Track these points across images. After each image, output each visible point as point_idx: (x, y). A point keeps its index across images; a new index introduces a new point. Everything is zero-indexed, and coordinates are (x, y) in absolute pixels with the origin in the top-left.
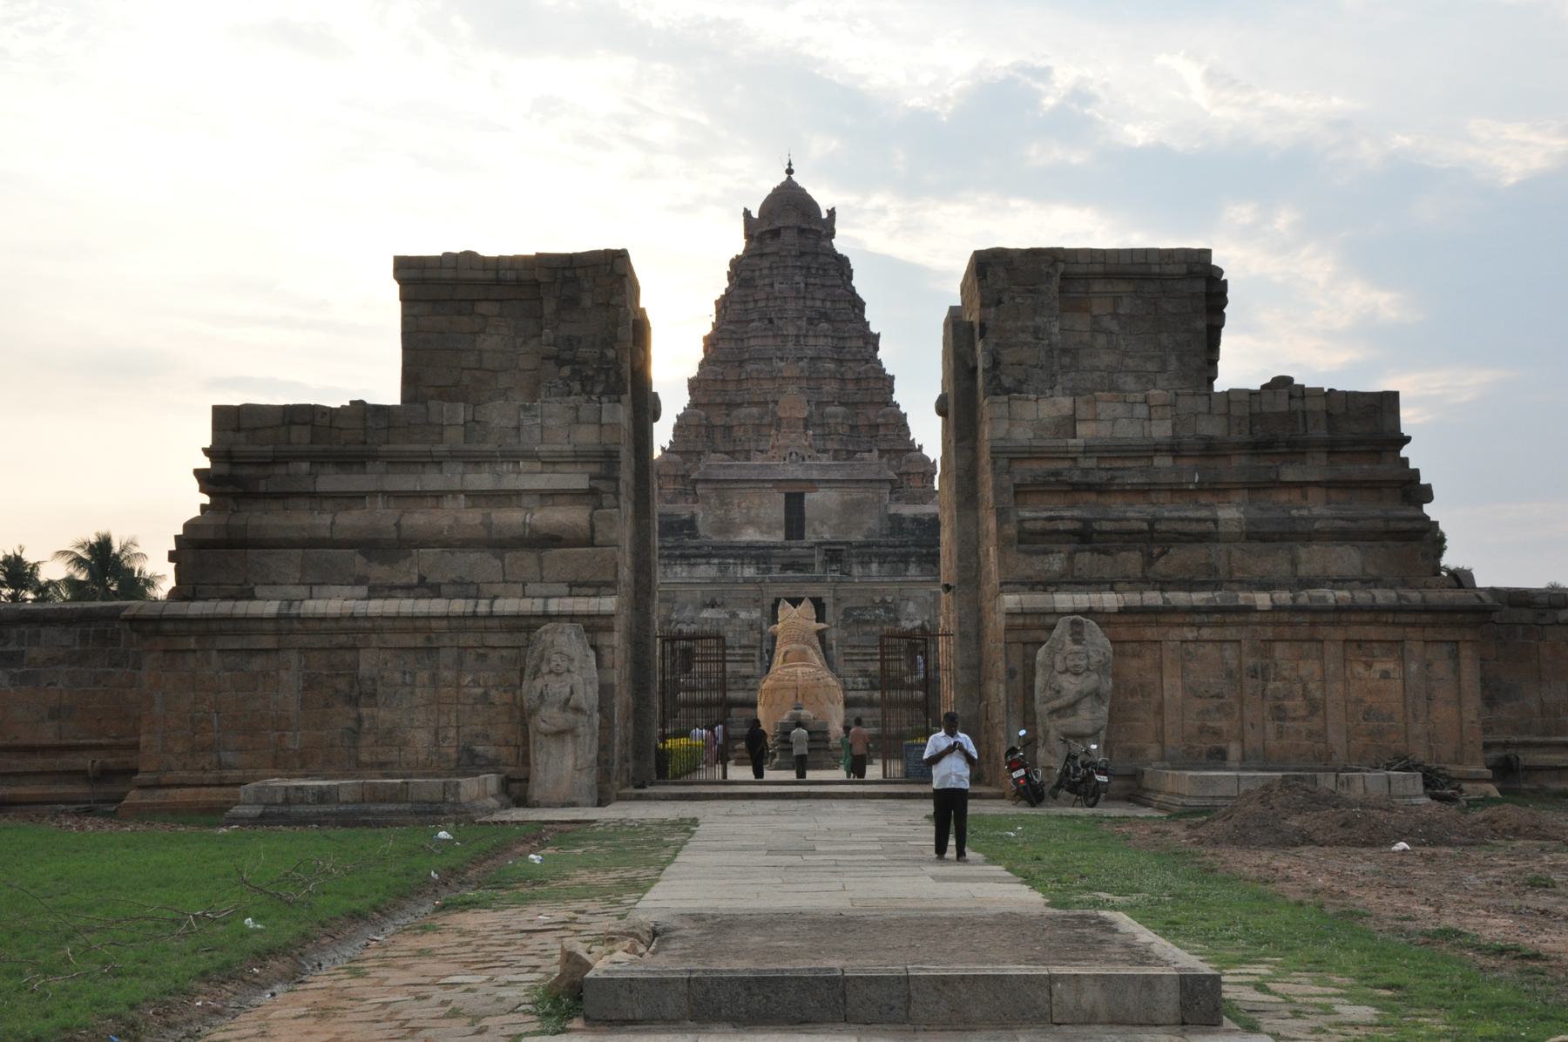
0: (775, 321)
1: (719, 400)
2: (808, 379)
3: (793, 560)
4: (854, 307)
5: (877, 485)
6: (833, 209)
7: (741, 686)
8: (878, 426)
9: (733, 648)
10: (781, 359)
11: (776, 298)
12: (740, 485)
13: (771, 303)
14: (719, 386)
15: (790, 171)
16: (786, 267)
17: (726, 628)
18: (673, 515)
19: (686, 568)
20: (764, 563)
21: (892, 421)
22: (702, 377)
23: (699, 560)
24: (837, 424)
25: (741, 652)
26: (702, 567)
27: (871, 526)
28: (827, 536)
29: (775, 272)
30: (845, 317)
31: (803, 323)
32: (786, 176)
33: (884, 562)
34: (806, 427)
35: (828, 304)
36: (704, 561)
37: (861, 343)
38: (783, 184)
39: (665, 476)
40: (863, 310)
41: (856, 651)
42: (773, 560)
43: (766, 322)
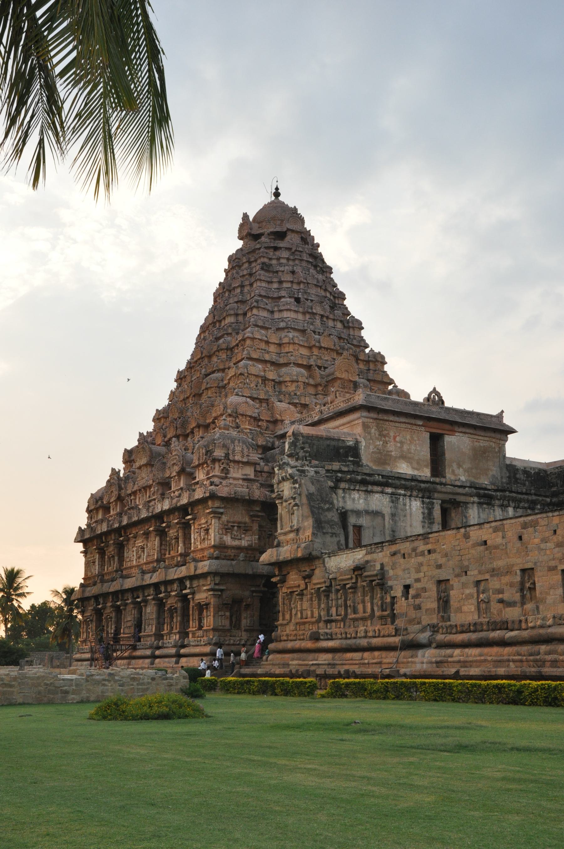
1: (267, 357)
3: (451, 497)
5: (498, 436)
10: (314, 332)
11: (299, 283)
12: (396, 419)
14: (263, 346)
15: (277, 194)
16: (302, 260)
18: (339, 440)
19: (363, 495)
20: (429, 498)
23: (376, 488)
26: (377, 495)
27: (494, 473)
28: (463, 478)
32: (273, 198)
33: (518, 507)
36: (379, 489)
38: (272, 202)
39: (242, 415)
42: (436, 495)
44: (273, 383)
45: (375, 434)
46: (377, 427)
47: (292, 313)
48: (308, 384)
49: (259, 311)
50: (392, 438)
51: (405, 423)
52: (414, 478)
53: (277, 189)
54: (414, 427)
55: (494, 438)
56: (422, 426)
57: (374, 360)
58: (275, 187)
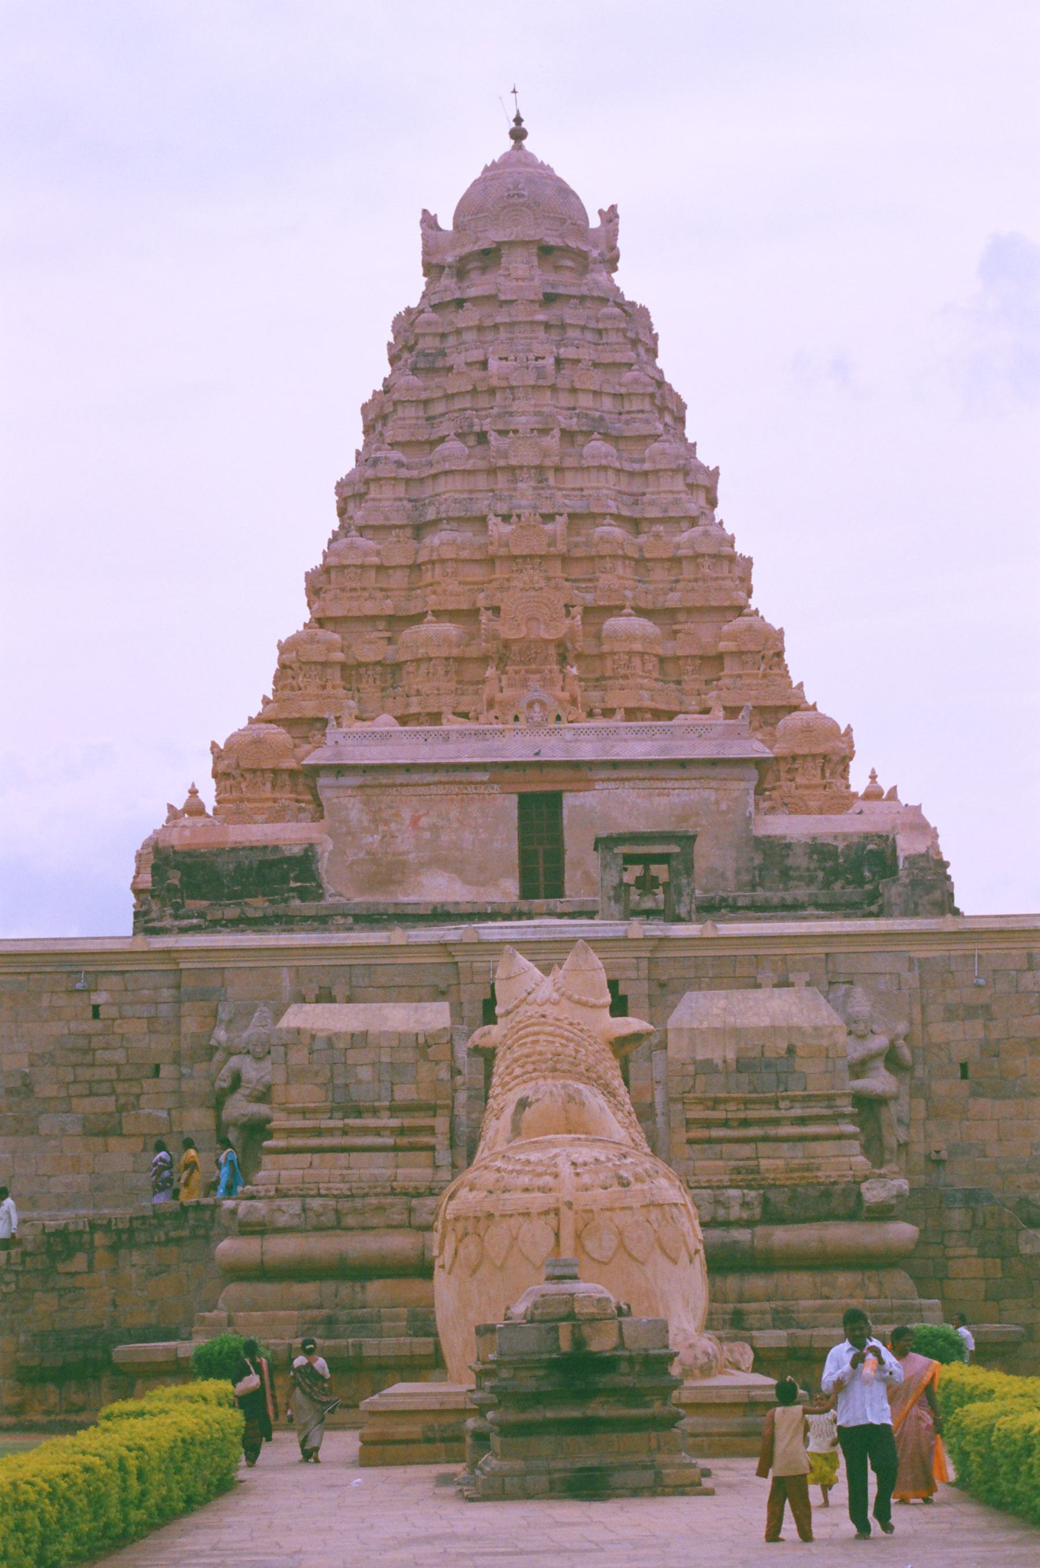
0: (493, 437)
1: (370, 608)
2: (565, 559)
4: (662, 409)
6: (613, 208)
7: (397, 1218)
8: (720, 658)
9: (375, 1112)
10: (506, 518)
11: (492, 391)
12: (416, 777)
13: (483, 402)
15: (518, 134)
17: (353, 1056)
21: (752, 647)
22: (333, 561)
24: (630, 653)
25: (395, 1122)
29: (490, 336)
30: (645, 430)
31: (552, 441)
34: (563, 659)
35: (607, 403)
37: (679, 484)
39: (254, 771)
40: (681, 420)
41: (719, 1114)
43: (472, 440)
44: (379, 669)
45: (360, 821)
46: (367, 803)
47: (458, 478)
48: (460, 660)
49: (381, 486)
50: (408, 822)
51: (440, 783)
52: (439, 910)
53: (518, 120)
54: (471, 789)
55: (714, 779)
56: (491, 782)
57: (690, 552)
58: (514, 116)
